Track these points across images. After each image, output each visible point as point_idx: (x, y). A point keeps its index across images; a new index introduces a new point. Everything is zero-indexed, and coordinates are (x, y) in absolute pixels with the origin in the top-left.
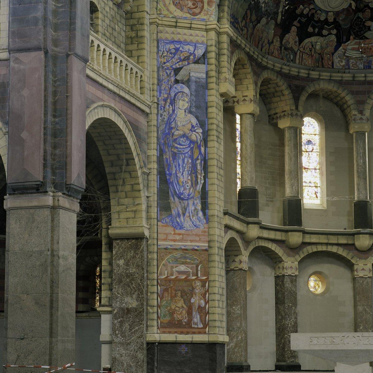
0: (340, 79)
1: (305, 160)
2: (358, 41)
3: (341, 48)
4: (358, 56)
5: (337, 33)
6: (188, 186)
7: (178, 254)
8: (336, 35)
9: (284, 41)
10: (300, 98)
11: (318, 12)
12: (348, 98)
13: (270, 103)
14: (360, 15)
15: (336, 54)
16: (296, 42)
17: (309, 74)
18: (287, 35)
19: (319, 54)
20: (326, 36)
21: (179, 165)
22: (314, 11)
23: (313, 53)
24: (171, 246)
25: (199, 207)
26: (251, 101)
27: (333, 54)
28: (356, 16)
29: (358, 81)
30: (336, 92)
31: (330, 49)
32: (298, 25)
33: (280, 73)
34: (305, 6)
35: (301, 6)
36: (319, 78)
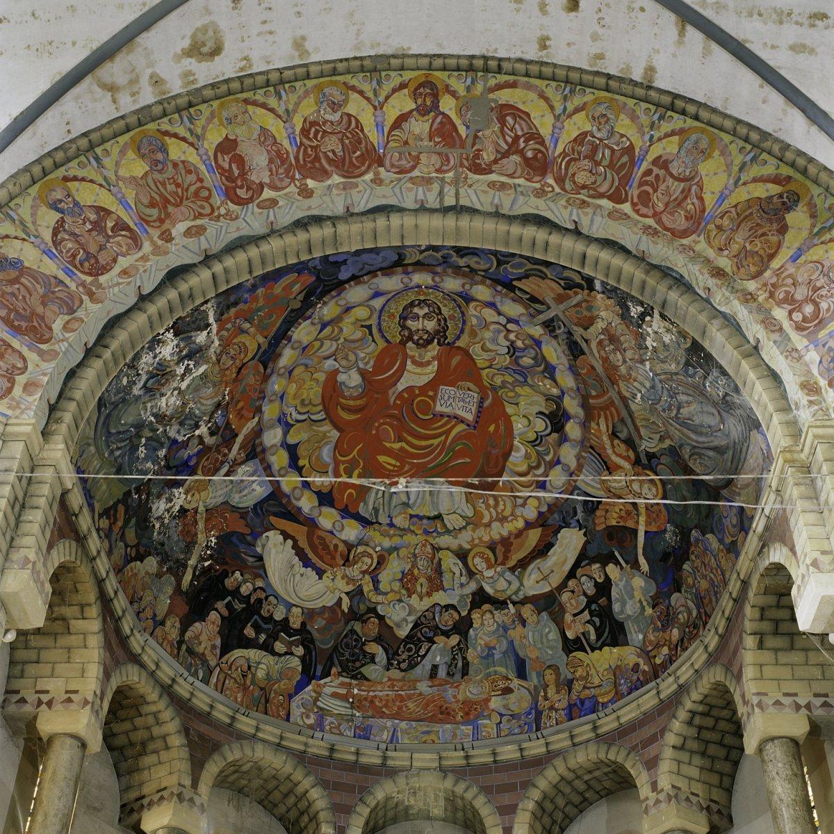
0: (302, 748)
2: (348, 680)
3: (310, 687)
4: (343, 711)
5: (305, 655)
8: (303, 659)
9: (188, 634)
10: (207, 766)
11: (271, 598)
12: (315, 794)
13: (130, 772)
14: (357, 626)
15: (298, 698)
16: (214, 647)
17: (233, 718)
18: (197, 624)
19: (262, 689)
20: (280, 655)
22: (263, 596)
23: (248, 682)
26: (86, 702)
27: (291, 697)
28: (349, 627)
29: (342, 761)
30: (288, 778)
31: (286, 685)
32: (225, 613)
33: (167, 690)
34: (247, 576)
35: (237, 574)
36: (254, 736)
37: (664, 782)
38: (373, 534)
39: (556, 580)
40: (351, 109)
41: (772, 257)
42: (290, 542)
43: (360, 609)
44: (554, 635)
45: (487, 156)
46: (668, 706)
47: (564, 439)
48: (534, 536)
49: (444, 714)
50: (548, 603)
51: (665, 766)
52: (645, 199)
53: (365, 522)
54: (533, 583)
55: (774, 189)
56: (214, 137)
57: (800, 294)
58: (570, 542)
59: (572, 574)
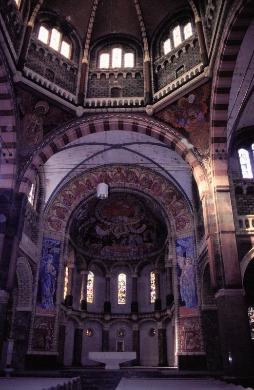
1: (88, 286)
7: (42, 319)
14: (111, 238)
31: (100, 248)
37: (156, 267)
38: (113, 223)
39: (142, 231)
40: (107, 172)
41: (171, 202)
43: (111, 235)
44: (142, 239)
45: (129, 180)
46: (157, 256)
47: (143, 213)
48: (139, 225)
49: (125, 251)
50: (141, 235)
51: (156, 264)
52: (153, 189)
53: (112, 222)
54: (138, 231)
55: (172, 191)
56: (86, 179)
57: (174, 209)
58: (144, 226)
59: (145, 231)
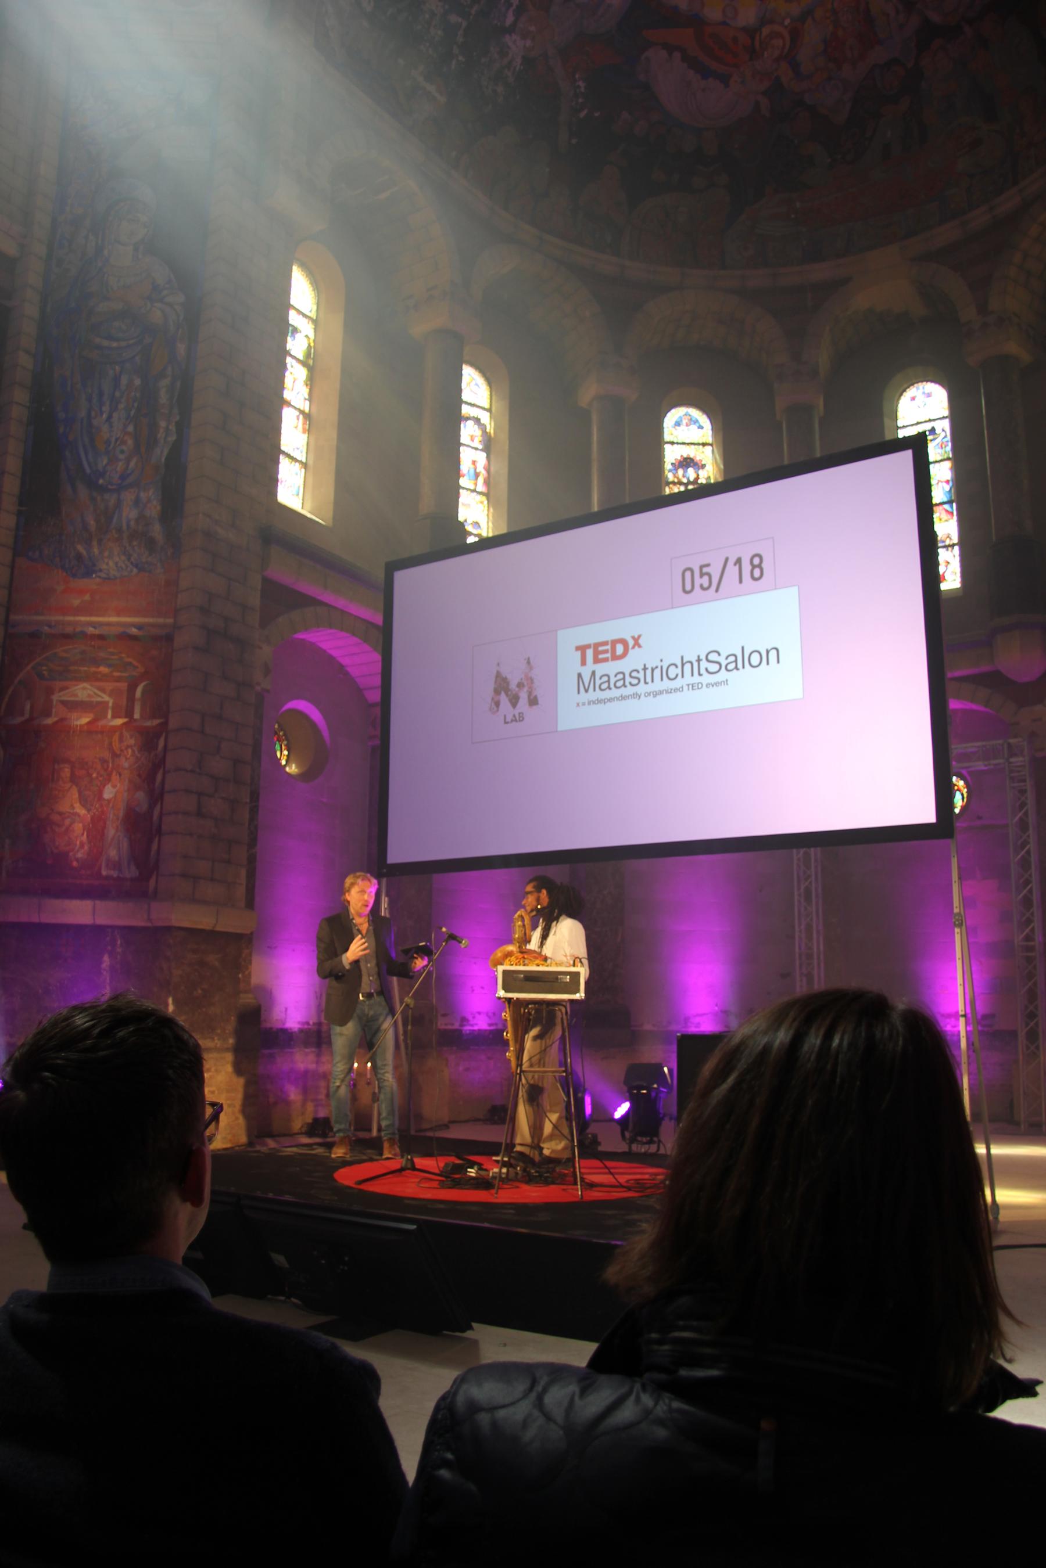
6: (122, 452)
21: (101, 394)
24: (50, 626)
25: (154, 510)
42: (677, 55)
